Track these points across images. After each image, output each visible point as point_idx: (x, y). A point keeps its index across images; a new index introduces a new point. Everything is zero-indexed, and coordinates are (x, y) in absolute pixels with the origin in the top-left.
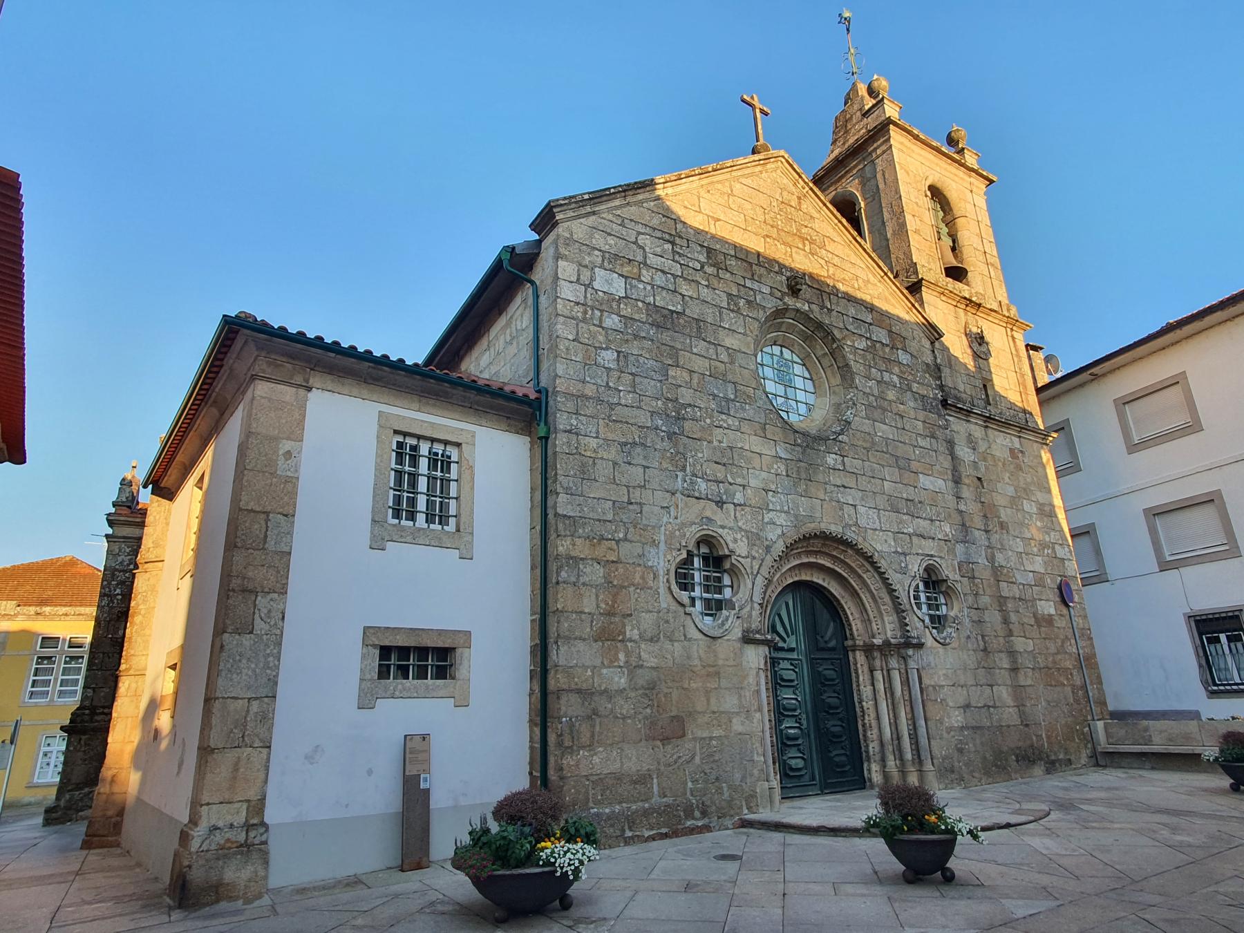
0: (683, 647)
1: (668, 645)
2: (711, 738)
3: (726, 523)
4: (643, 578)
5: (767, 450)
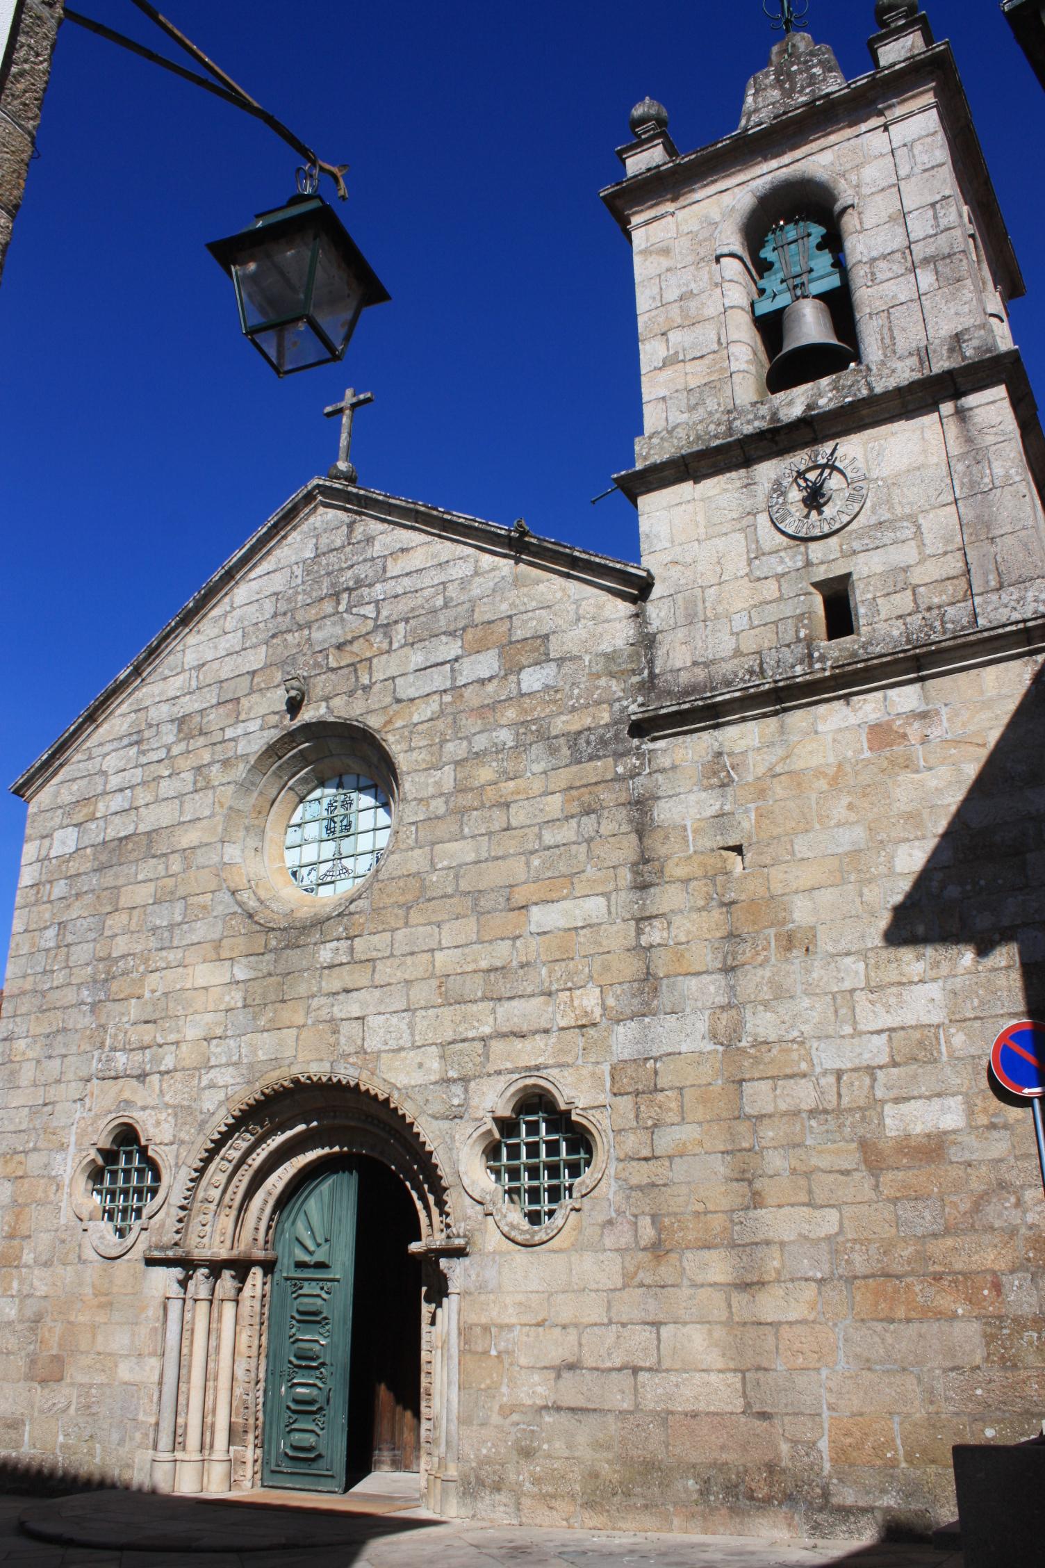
2: (91, 1386)
4: (45, 1192)
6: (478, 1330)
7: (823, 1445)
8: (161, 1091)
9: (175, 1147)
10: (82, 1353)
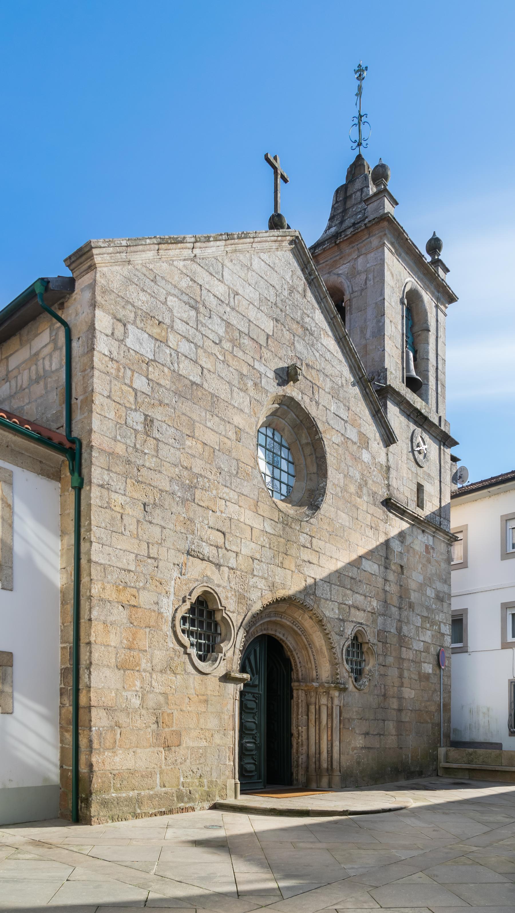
0: (183, 679)
1: (172, 677)
3: (221, 582)
5: (257, 524)
6: (347, 720)
7: (410, 755)
8: (229, 579)
9: (235, 615)
10: (191, 729)
